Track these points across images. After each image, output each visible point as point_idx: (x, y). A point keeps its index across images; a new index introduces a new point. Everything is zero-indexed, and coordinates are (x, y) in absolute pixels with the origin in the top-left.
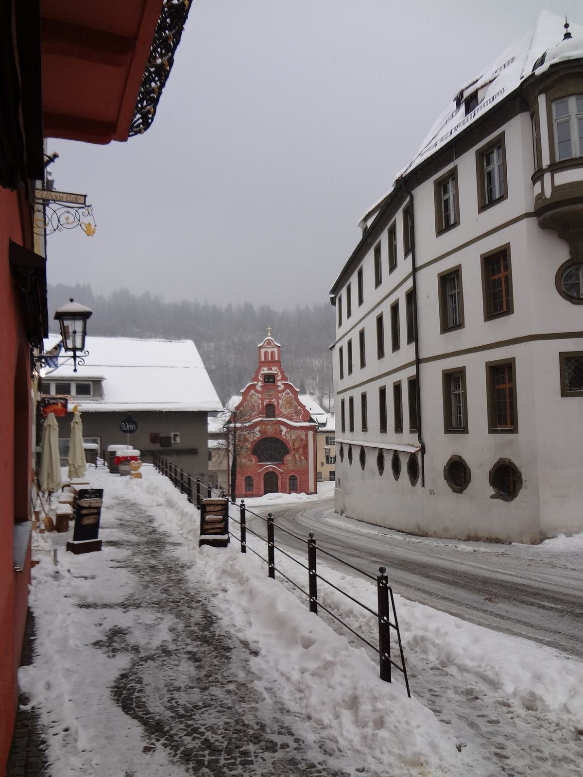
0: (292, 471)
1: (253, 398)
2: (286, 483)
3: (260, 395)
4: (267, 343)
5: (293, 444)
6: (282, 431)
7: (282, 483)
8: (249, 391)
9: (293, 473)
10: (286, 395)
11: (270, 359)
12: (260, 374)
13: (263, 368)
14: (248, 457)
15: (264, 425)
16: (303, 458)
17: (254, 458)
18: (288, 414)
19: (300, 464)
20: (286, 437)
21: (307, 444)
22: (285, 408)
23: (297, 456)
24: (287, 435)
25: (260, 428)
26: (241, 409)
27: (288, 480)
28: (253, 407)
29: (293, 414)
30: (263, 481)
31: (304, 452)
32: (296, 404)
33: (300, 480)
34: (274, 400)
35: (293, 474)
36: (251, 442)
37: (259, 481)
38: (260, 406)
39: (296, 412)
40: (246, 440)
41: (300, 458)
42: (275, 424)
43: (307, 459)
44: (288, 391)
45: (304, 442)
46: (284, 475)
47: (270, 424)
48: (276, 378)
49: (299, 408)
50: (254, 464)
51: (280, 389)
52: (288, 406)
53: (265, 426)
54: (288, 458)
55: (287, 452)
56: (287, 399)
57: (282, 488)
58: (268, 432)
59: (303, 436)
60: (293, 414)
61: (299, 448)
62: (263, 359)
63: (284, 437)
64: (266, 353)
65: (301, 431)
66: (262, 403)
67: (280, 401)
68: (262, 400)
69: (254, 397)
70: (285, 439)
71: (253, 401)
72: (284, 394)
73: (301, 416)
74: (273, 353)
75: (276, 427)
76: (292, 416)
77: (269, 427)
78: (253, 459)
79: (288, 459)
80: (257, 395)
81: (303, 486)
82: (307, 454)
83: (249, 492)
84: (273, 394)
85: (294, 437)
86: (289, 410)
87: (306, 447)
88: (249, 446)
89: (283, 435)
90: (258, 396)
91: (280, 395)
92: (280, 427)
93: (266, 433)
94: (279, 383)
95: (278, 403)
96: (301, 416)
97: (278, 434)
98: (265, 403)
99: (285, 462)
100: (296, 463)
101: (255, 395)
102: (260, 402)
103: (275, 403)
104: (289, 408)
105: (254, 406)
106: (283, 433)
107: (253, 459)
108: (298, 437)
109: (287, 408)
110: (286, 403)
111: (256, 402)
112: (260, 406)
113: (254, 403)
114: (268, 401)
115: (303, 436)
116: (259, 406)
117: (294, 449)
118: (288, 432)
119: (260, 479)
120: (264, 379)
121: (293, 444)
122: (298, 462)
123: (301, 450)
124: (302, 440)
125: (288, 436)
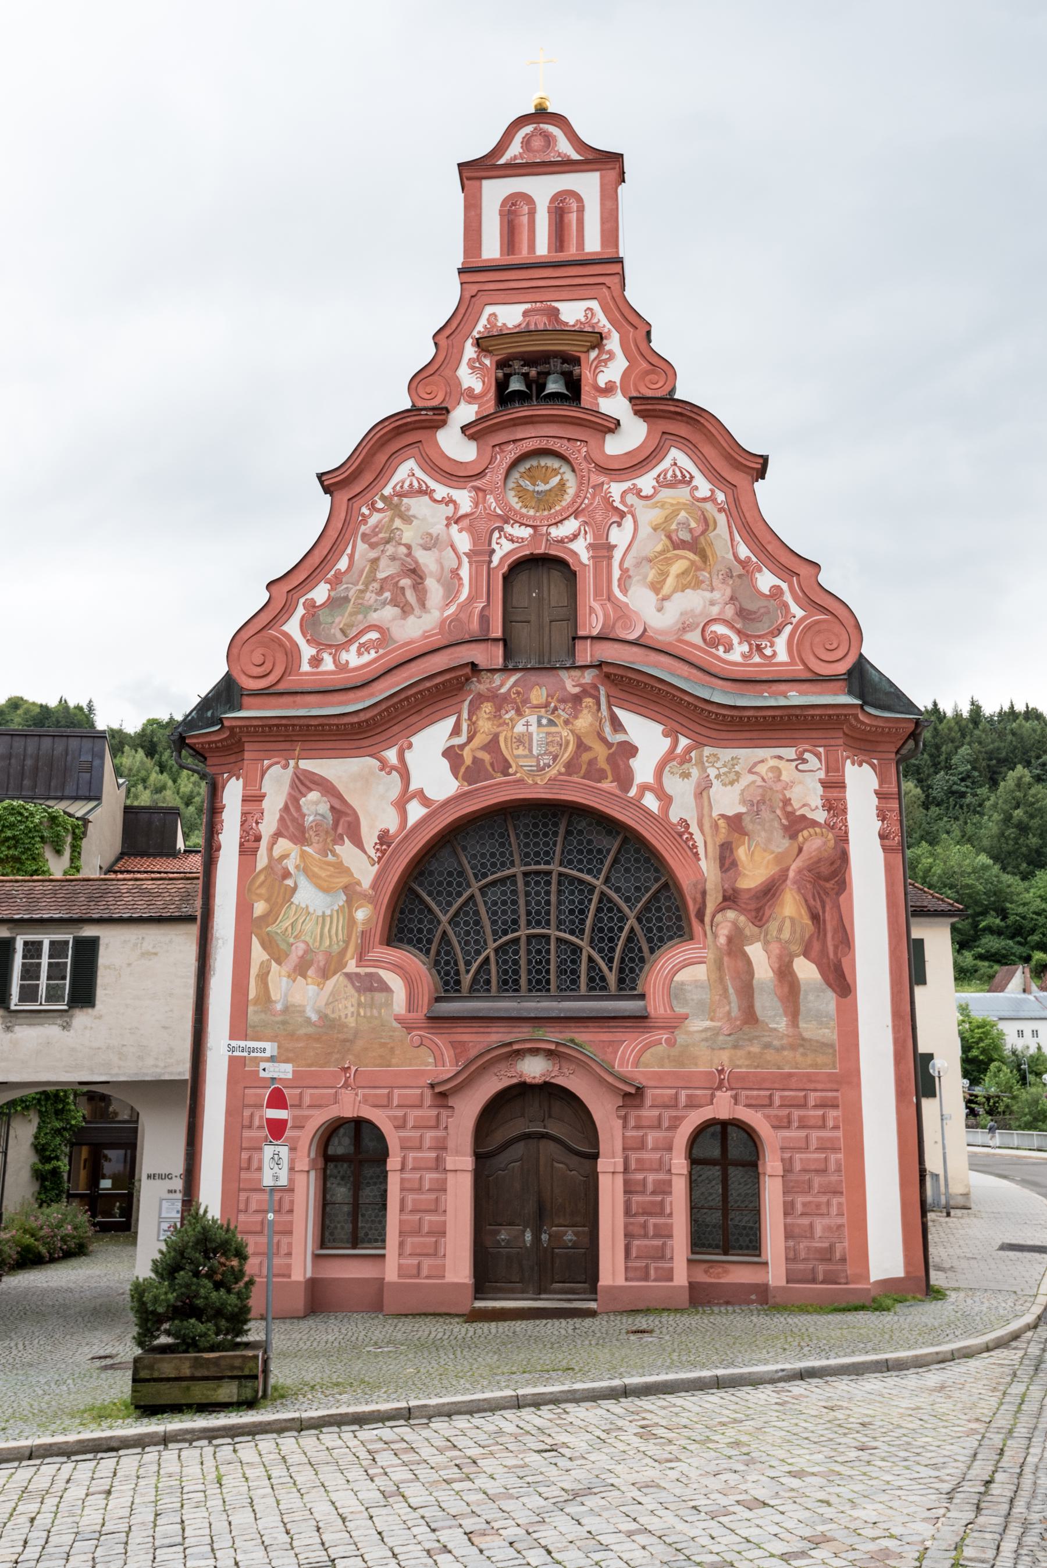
0: (719, 1081)
1: (407, 519)
2: (664, 1189)
3: (464, 499)
4: (526, 142)
5: (727, 860)
6: (630, 750)
7: (629, 1189)
8: (384, 473)
9: (724, 1097)
10: (666, 494)
11: (542, 248)
12: (470, 351)
13: (489, 310)
14: (352, 967)
15: (487, 707)
16: (806, 970)
17: (397, 968)
18: (685, 628)
19: (781, 1024)
20: (666, 799)
21: (843, 857)
22: (656, 587)
23: (756, 952)
24: (673, 784)
25: (456, 731)
26: (320, 593)
27: (679, 1163)
28: (406, 582)
29: (720, 629)
30: (467, 1162)
31: (815, 917)
32: (744, 552)
33: (788, 1169)
34: (571, 526)
35: (723, 1108)
36: (384, 838)
37: (438, 1165)
38: (465, 573)
39: (743, 613)
40: (344, 822)
41: (785, 973)
42: (577, 699)
43: (840, 981)
44: (677, 458)
45: (815, 844)
46: (648, 1113)
47: (538, 695)
48: (587, 375)
49: (766, 581)
50: (398, 1019)
51: (615, 446)
52: (677, 567)
53: (497, 716)
54: (684, 974)
55: (669, 916)
56: (668, 519)
57: (628, 1235)
58: (521, 762)
59: (807, 794)
60: (720, 629)
61: (770, 891)
62: (491, 249)
63: (650, 802)
64: (513, 211)
65: (790, 753)
66: (481, 553)
67: (619, 537)
68: (482, 529)
69: (418, 506)
70: (661, 821)
71: (408, 534)
72: (646, 482)
73: (781, 643)
74: (562, 209)
75: (584, 721)
76: (715, 641)
77: (529, 725)
78: (382, 973)
79: (683, 976)
80: (441, 491)
81: (819, 1224)
82: (845, 940)
83: (349, 1270)
84: (562, 485)
85: (727, 800)
86: (693, 601)
87: (831, 877)
88: (362, 867)
89: (644, 788)
90: (449, 501)
91: (616, 489)
92: (617, 725)
93: (505, 767)
94: (616, 406)
95: (603, 550)
96: (781, 643)
97: (601, 776)
98: (503, 550)
99: (656, 1006)
100: (750, 1016)
101: (428, 492)
102: (463, 542)
103: (580, 547)
104: (690, 581)
105: (416, 573)
106: (643, 769)
107: (395, 983)
108: (767, 800)
109: (670, 581)
110: (660, 543)
111: (431, 543)
112: (465, 573)
113: (420, 555)
114: (526, 532)
115: (807, 794)
116: (455, 573)
117: (730, 899)
118: (685, 759)
119: (441, 1147)
120: (501, 385)
121: (727, 860)
122: (768, 1006)
123: (790, 906)
124: (796, 824)
125: (681, 789)
